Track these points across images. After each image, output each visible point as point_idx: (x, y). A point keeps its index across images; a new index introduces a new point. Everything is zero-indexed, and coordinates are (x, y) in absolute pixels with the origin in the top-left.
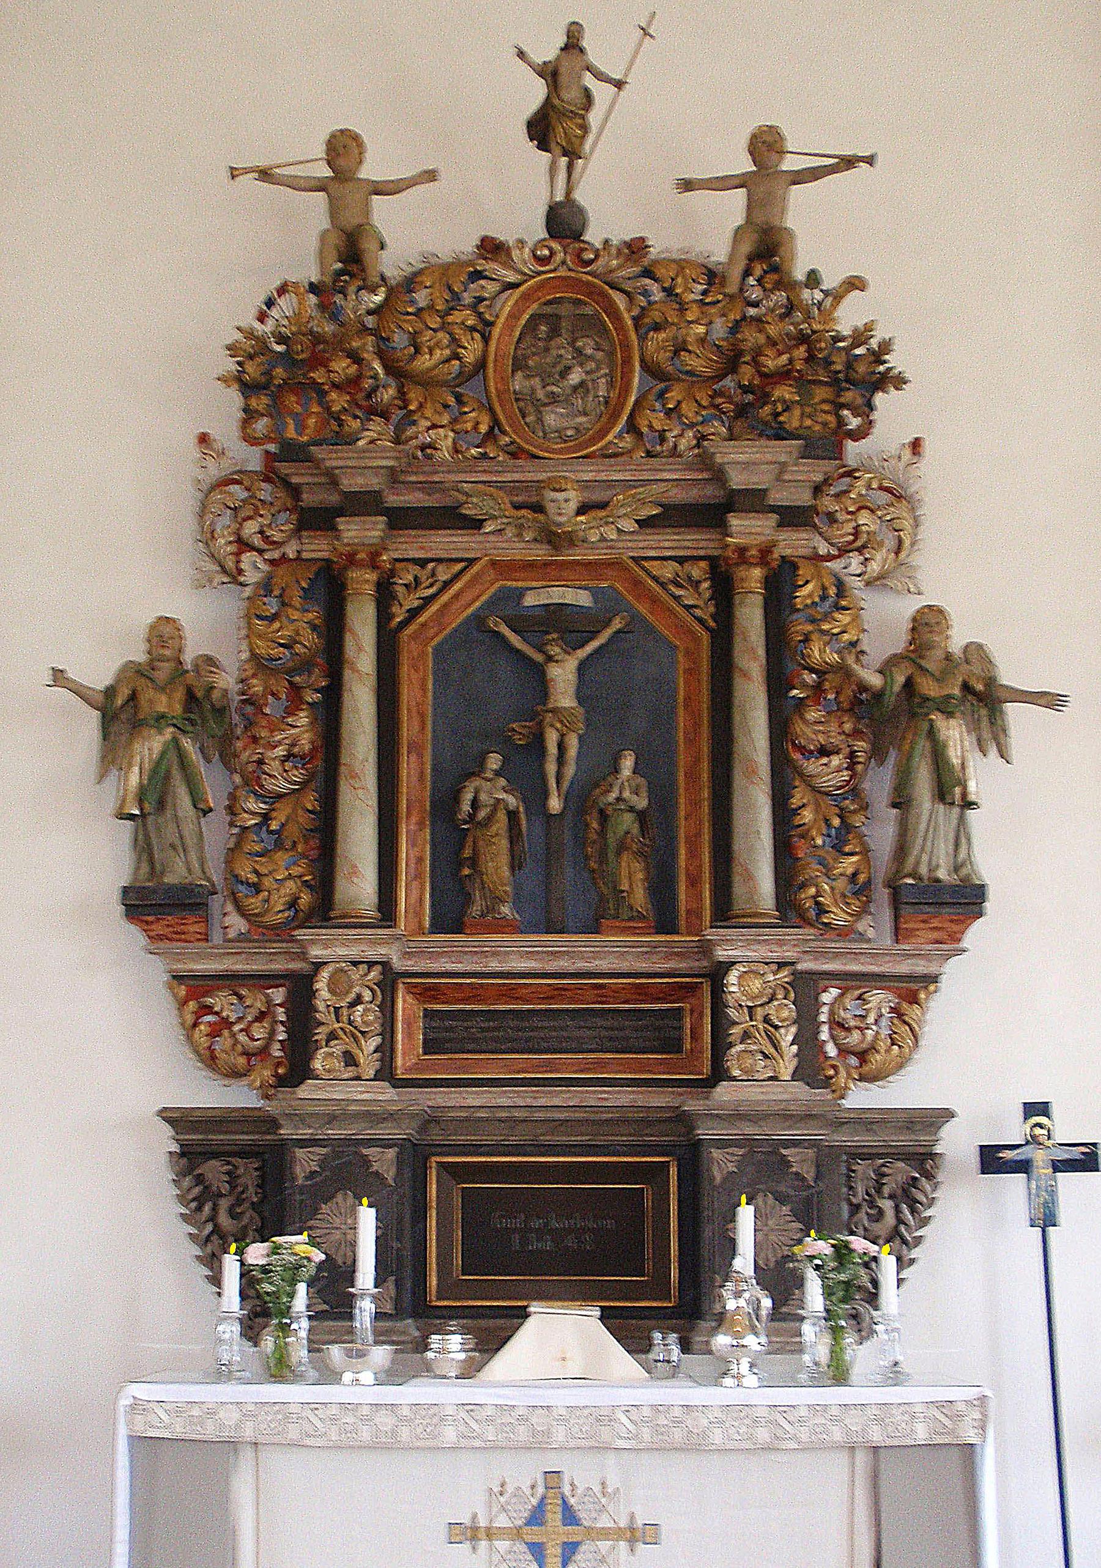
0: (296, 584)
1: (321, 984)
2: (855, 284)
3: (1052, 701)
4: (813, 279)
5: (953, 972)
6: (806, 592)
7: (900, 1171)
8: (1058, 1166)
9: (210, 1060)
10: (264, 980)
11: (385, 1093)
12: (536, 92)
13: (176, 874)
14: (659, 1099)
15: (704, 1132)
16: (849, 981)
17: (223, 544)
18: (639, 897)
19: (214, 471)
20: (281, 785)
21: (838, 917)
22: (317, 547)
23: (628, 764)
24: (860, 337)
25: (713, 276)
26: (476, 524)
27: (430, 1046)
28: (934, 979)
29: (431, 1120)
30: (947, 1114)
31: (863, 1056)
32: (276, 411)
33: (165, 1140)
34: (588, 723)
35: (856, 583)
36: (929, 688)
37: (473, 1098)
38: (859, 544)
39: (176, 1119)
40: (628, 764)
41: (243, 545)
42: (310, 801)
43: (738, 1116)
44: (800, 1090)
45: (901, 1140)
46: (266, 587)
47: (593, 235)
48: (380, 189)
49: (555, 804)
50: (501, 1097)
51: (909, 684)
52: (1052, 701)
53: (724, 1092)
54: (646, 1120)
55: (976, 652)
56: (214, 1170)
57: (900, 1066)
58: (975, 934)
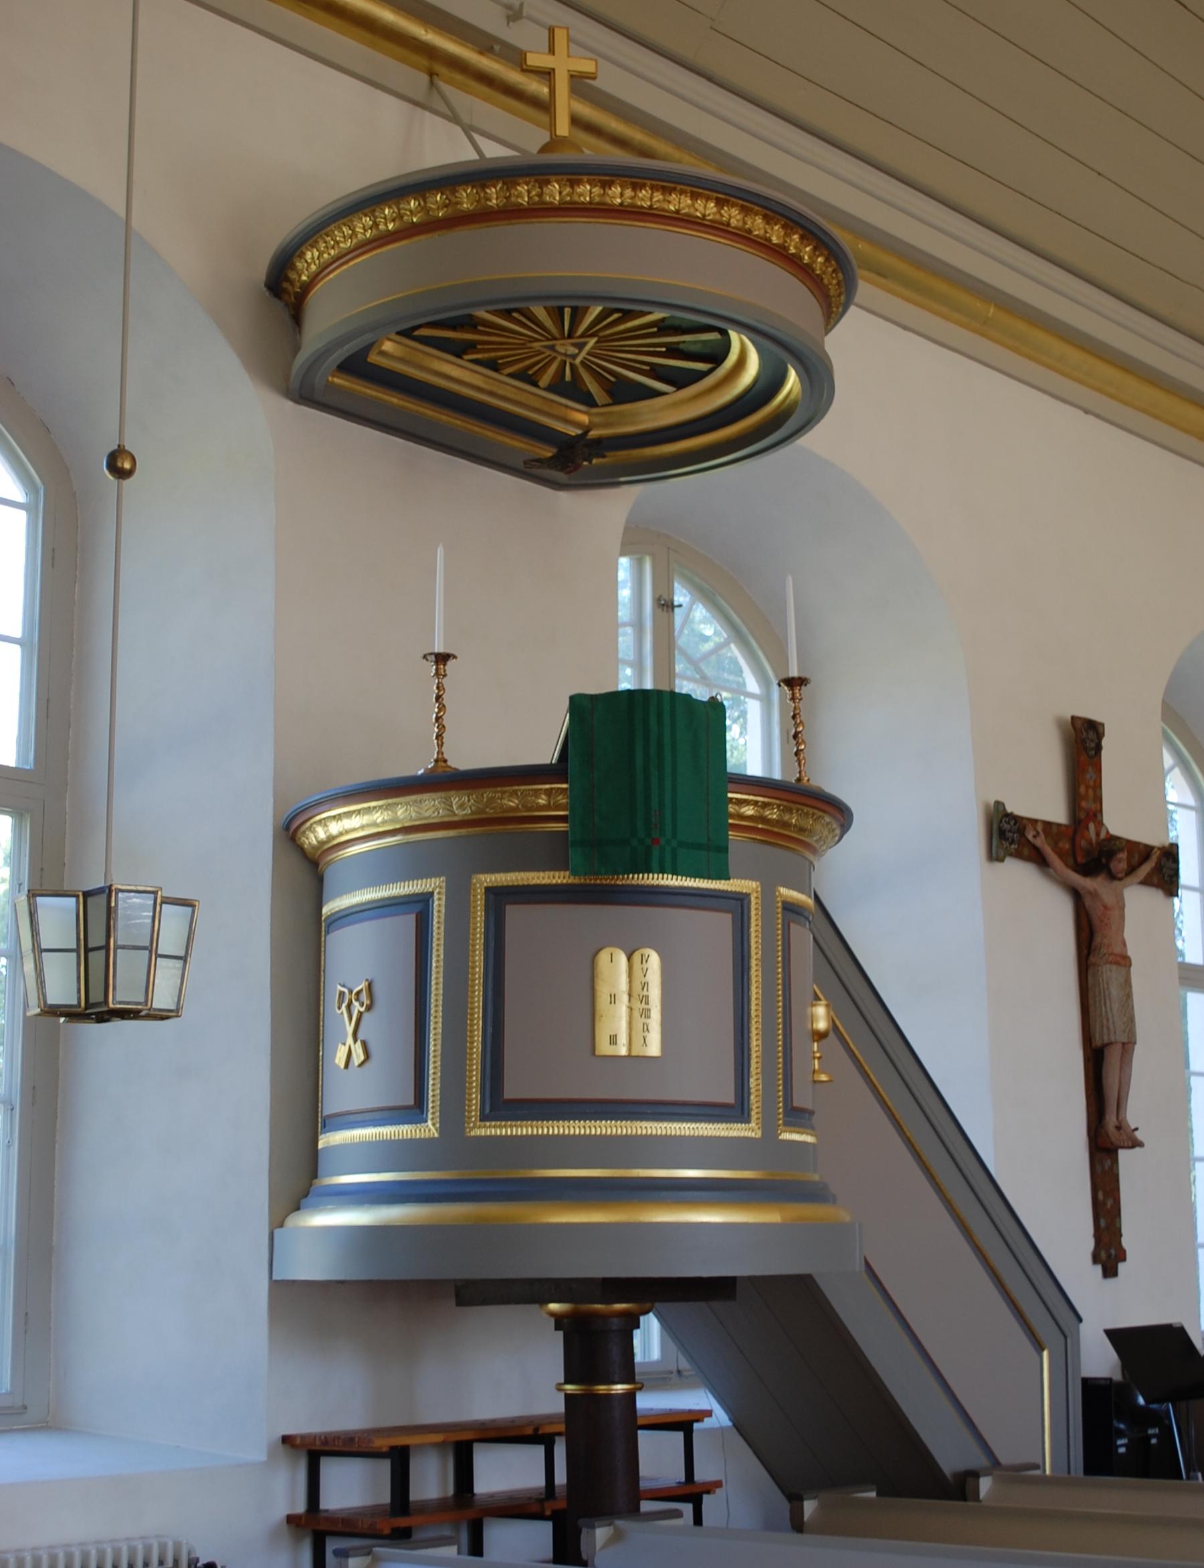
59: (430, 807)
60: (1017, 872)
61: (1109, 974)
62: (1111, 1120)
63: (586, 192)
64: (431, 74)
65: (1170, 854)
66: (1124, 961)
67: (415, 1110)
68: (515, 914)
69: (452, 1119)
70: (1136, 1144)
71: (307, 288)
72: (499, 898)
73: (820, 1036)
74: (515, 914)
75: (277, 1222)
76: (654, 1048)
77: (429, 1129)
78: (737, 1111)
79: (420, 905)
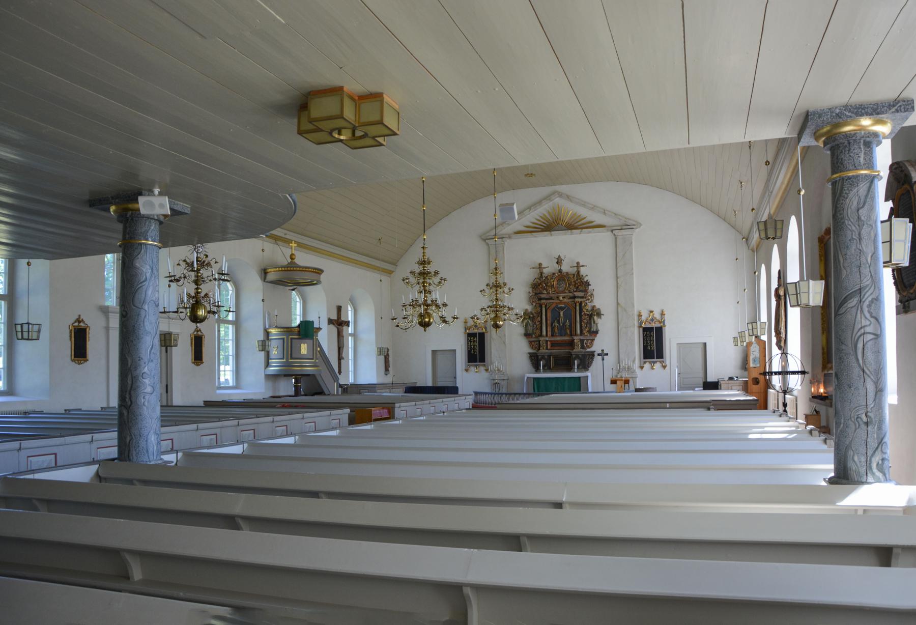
0: (538, 305)
1: (541, 342)
2: (587, 276)
3: (603, 315)
4: (582, 276)
5: (596, 338)
6: (583, 304)
7: (591, 356)
8: (604, 355)
9: (532, 348)
10: (537, 341)
11: (547, 351)
12: (557, 261)
13: (528, 332)
14: (570, 350)
15: (573, 354)
16: (587, 340)
17: (531, 302)
18: (569, 332)
19: (530, 295)
20: (537, 324)
21: (586, 334)
22: (539, 302)
23: (568, 321)
24: (587, 281)
25: (574, 275)
26: (554, 299)
27: (551, 346)
28: (594, 339)
29: (551, 352)
30: (595, 351)
31: (588, 346)
32: (535, 290)
33: (529, 355)
34: (564, 318)
35: (588, 303)
36: (593, 313)
37: (555, 351)
38: (589, 300)
39: (529, 353)
40: (568, 321)
41: (533, 302)
42: (540, 325)
43: (575, 352)
44: (582, 350)
45: (591, 353)
46: (535, 306)
47: (563, 272)
48: (545, 268)
49: (561, 325)
50: (557, 351)
51: (592, 313)
52: (603, 315)
53: (574, 350)
54: (567, 352)
55: (599, 309)
56: (533, 358)
57: (592, 347)
58: (598, 335)
59: (282, 330)
60: (331, 326)
61: (341, 338)
62: (341, 356)
63: (301, 269)
64: (276, 240)
65: (349, 322)
66: (343, 337)
67: (283, 359)
68: (293, 340)
69: (287, 359)
70: (343, 359)
71: (268, 272)
72: (292, 339)
73: (319, 351)
74: (293, 340)
75: (265, 369)
76: (306, 353)
77: (285, 360)
78: (313, 359)
79: (283, 339)
